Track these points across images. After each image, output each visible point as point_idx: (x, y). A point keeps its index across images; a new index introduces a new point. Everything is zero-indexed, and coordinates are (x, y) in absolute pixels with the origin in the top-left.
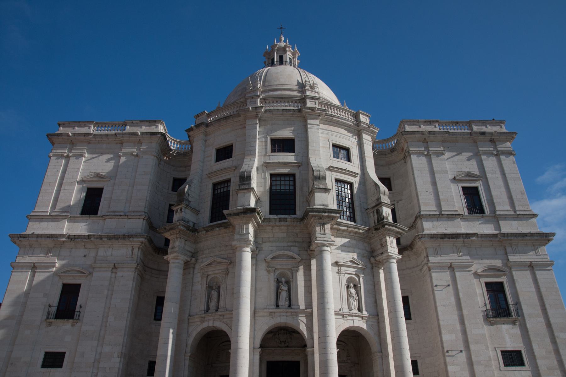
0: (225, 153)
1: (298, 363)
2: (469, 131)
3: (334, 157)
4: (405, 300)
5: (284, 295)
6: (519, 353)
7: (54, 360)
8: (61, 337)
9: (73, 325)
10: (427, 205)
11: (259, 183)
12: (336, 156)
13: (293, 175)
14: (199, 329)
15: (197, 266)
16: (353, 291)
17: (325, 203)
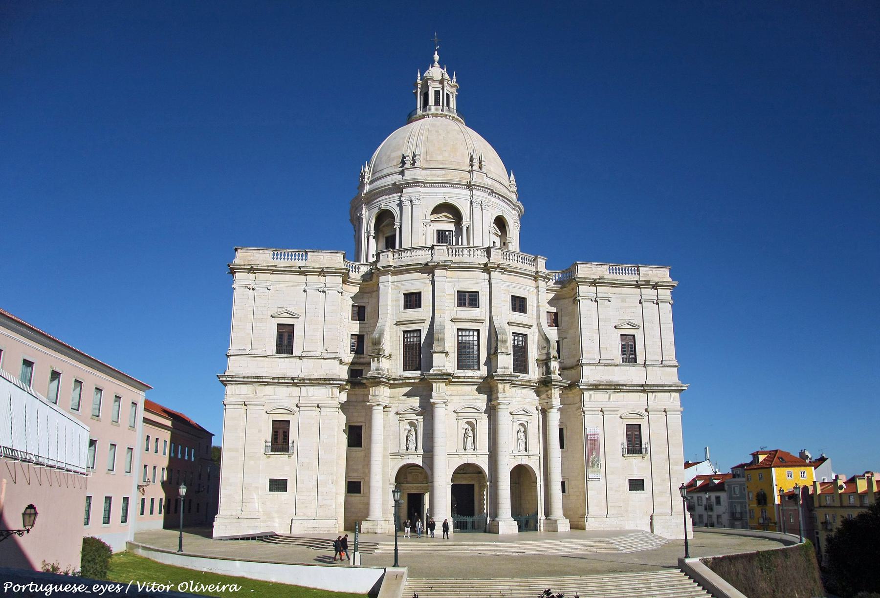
0: (413, 300)
1: (473, 485)
2: (636, 278)
3: (514, 309)
4: (561, 431)
5: (470, 440)
6: (642, 481)
7: (278, 485)
8: (279, 466)
9: (290, 456)
10: (589, 351)
11: (451, 344)
12: (514, 309)
13: (478, 331)
14: (401, 464)
15: (393, 410)
16: (522, 435)
17: (506, 366)
